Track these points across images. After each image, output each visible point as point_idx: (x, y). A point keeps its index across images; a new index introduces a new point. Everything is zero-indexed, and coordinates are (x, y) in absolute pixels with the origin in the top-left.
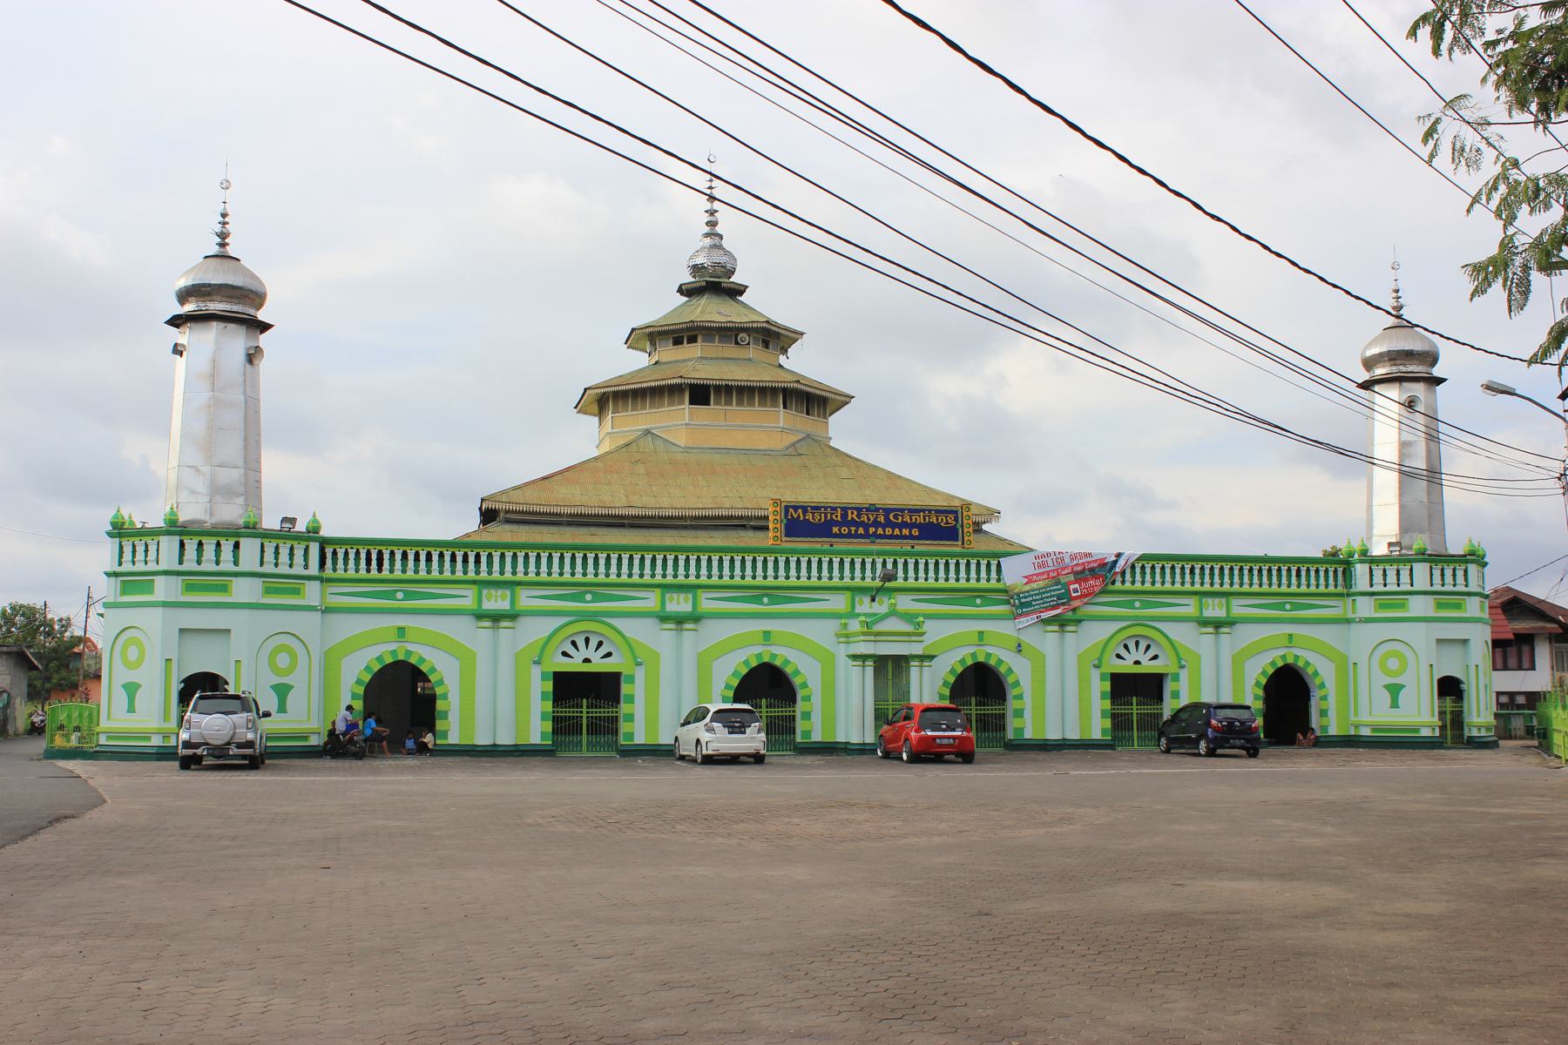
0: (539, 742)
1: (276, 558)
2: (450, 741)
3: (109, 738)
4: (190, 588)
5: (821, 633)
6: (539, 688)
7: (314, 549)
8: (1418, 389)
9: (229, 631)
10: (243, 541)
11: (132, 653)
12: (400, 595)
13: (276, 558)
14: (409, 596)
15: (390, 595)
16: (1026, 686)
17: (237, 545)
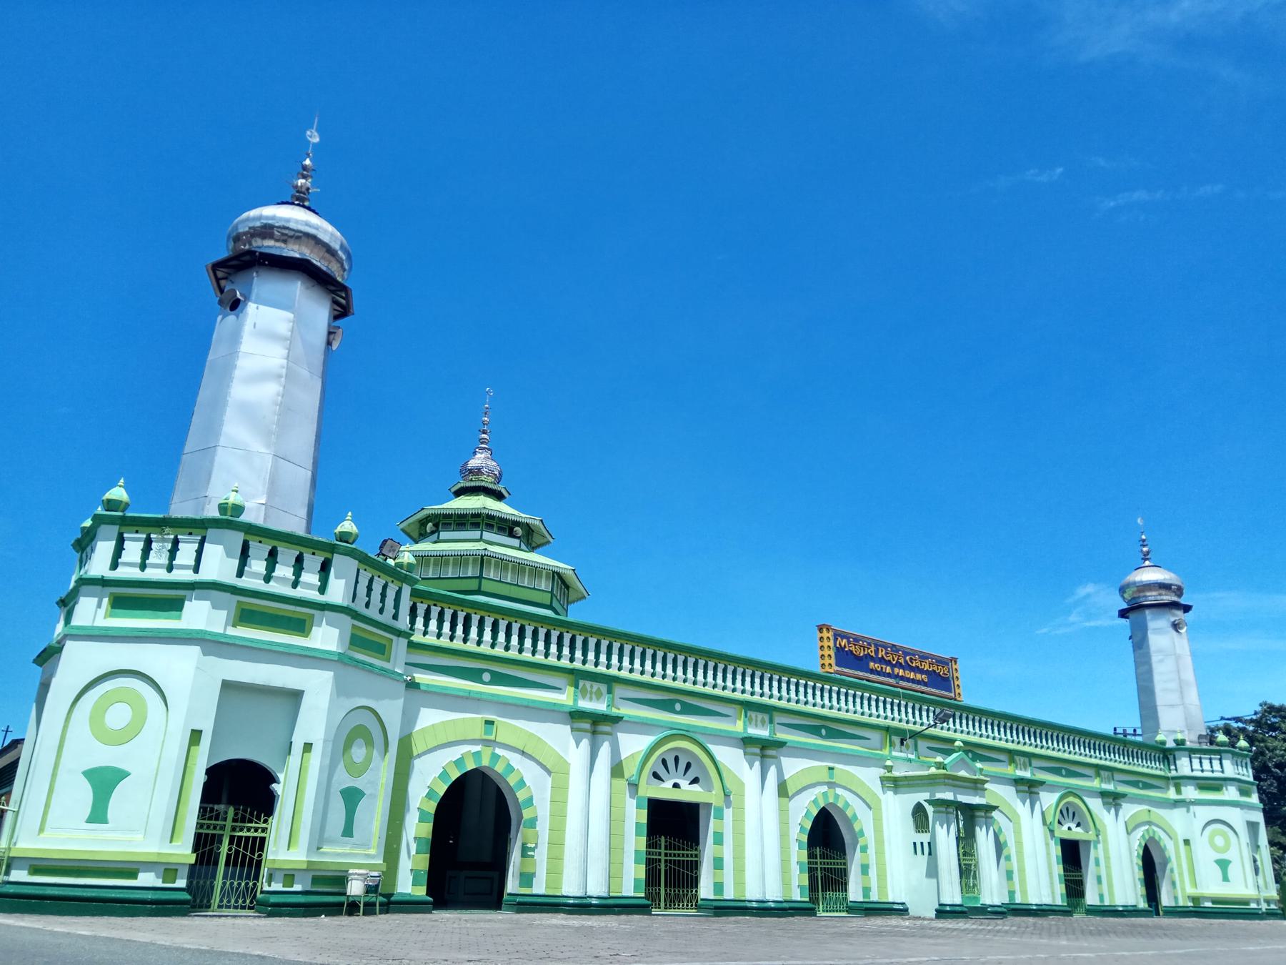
0: (632, 894)
1: (369, 595)
2: (535, 891)
3: (35, 870)
4: (246, 617)
5: (869, 776)
6: (636, 816)
7: (407, 591)
8: (1179, 614)
9: (296, 696)
10: (338, 560)
11: (118, 716)
12: (487, 677)
13: (369, 595)
14: (498, 679)
15: (474, 675)
16: (869, 837)
17: (325, 568)
